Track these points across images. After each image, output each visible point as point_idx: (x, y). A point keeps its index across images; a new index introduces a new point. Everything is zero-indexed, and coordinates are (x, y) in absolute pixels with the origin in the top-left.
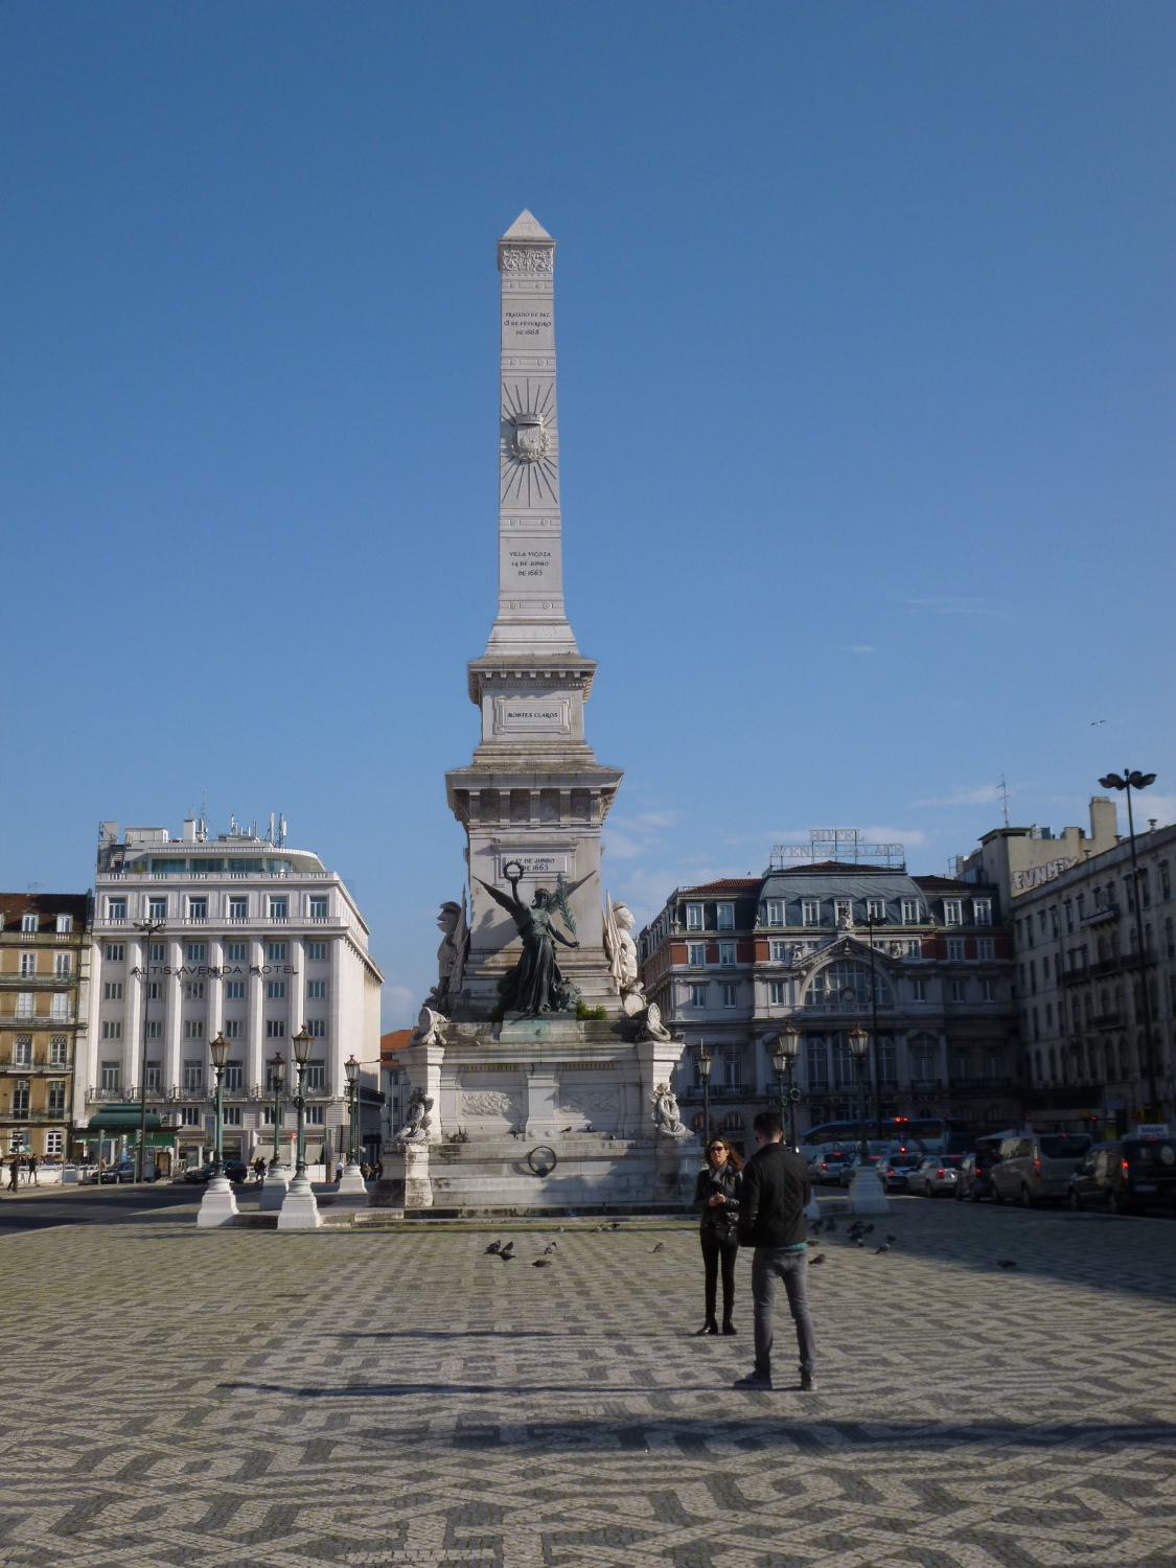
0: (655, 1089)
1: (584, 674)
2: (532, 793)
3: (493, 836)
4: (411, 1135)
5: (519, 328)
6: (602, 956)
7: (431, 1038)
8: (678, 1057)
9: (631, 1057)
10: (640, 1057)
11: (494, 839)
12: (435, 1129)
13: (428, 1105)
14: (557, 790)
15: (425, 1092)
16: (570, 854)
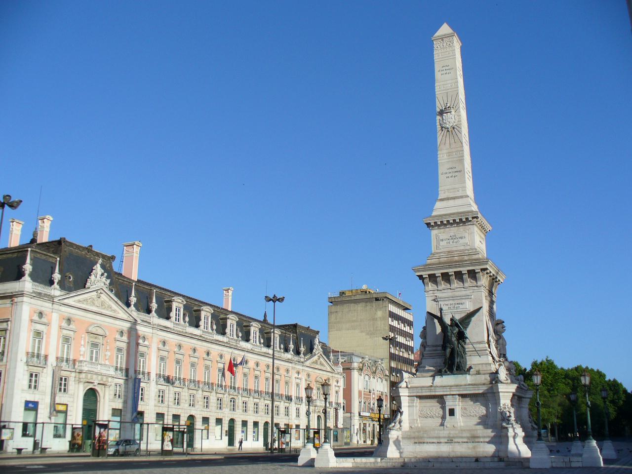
0: (501, 405)
1: (473, 218)
2: (450, 274)
3: (435, 295)
4: (394, 426)
5: (443, 72)
6: (487, 345)
7: (403, 384)
8: (514, 391)
9: (490, 391)
10: (495, 391)
11: (436, 296)
12: (406, 425)
13: (401, 413)
14: (460, 272)
15: (401, 409)
16: (470, 300)
